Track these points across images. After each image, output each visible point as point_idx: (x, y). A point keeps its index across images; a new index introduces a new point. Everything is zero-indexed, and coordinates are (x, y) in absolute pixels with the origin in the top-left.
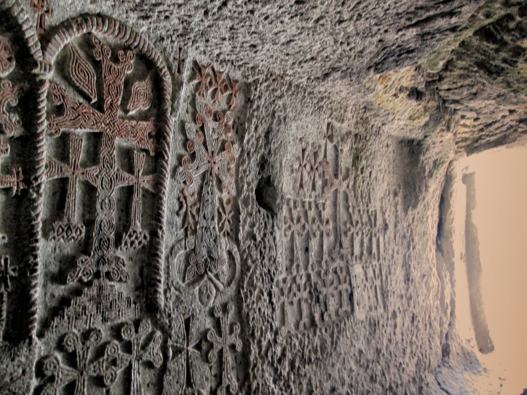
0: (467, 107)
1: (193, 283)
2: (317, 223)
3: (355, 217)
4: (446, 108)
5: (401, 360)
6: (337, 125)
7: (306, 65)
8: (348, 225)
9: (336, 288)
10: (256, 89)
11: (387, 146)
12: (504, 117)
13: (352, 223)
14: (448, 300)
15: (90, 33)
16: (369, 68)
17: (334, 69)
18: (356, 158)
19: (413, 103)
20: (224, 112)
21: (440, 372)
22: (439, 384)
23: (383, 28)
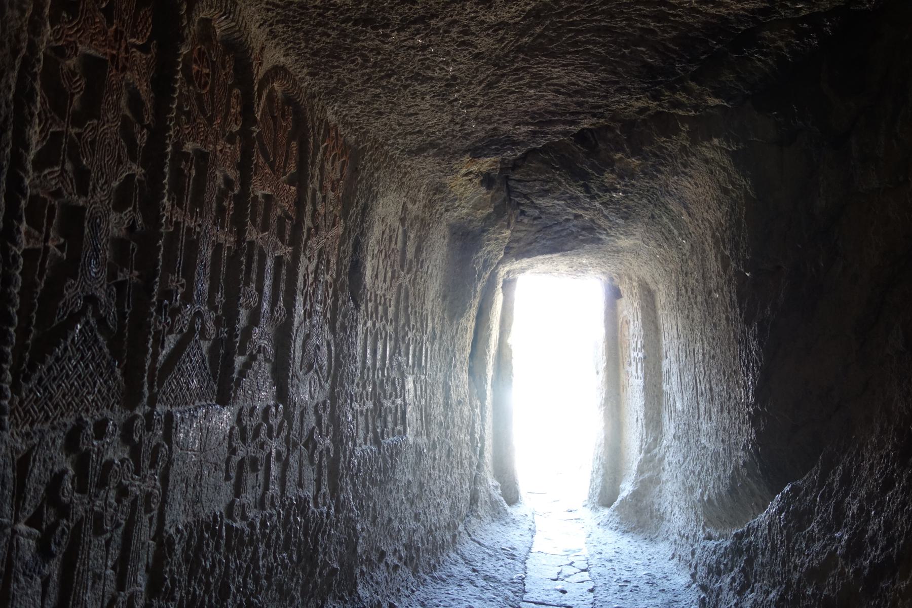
0: (532, 202)
1: (306, 373)
2: (384, 322)
3: (412, 322)
4: (511, 200)
5: (438, 500)
6: (410, 206)
7: (409, 137)
8: (407, 329)
9: (393, 403)
10: (363, 158)
11: (444, 237)
12: (568, 220)
13: (409, 327)
14: (477, 436)
15: (273, 88)
16: (465, 152)
17: (432, 145)
18: (419, 250)
19: (483, 190)
20: (338, 181)
21: (470, 522)
22: (470, 535)
23: (504, 119)
